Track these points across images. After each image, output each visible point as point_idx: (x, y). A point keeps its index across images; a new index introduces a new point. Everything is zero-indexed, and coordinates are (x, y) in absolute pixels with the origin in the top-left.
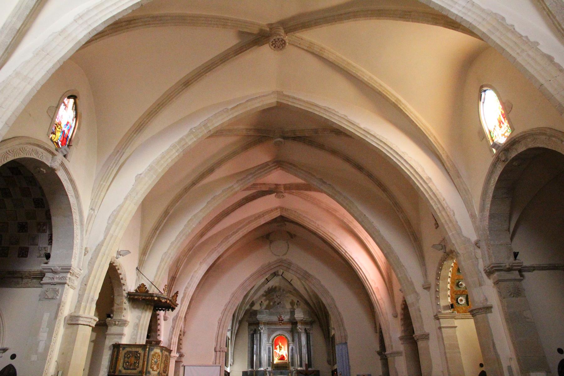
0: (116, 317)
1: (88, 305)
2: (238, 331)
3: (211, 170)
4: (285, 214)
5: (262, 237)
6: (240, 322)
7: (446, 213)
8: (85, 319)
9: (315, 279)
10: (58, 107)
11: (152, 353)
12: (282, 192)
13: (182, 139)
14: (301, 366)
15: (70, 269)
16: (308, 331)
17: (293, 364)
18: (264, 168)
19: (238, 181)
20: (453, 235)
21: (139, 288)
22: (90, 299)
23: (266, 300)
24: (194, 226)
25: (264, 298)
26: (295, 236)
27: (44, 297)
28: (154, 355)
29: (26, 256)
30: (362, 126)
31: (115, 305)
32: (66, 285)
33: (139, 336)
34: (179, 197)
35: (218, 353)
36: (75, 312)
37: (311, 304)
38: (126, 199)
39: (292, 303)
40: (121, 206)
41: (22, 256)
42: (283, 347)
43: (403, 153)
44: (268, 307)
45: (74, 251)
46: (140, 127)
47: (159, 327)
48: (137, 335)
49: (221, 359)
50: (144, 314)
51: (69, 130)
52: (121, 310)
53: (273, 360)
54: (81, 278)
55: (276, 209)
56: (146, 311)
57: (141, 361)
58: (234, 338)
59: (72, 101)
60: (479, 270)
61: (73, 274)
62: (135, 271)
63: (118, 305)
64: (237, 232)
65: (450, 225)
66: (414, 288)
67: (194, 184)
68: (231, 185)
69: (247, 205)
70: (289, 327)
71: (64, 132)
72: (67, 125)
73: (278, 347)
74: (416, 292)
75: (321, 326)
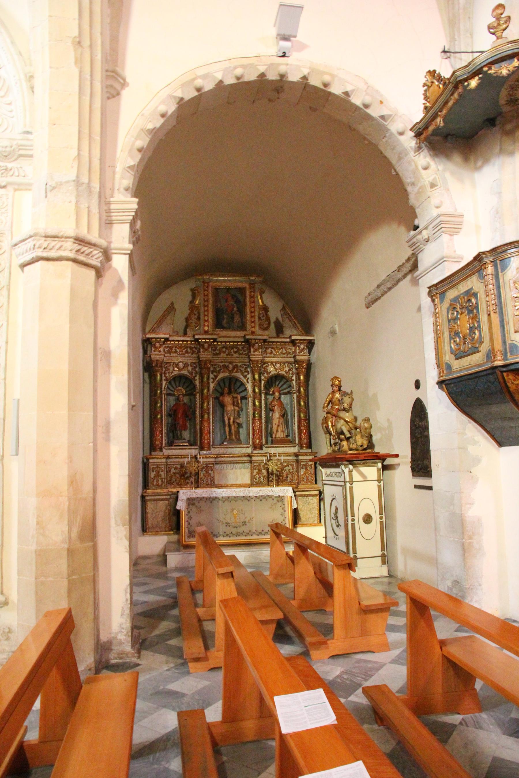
57: (484, 318)
63: (413, 184)
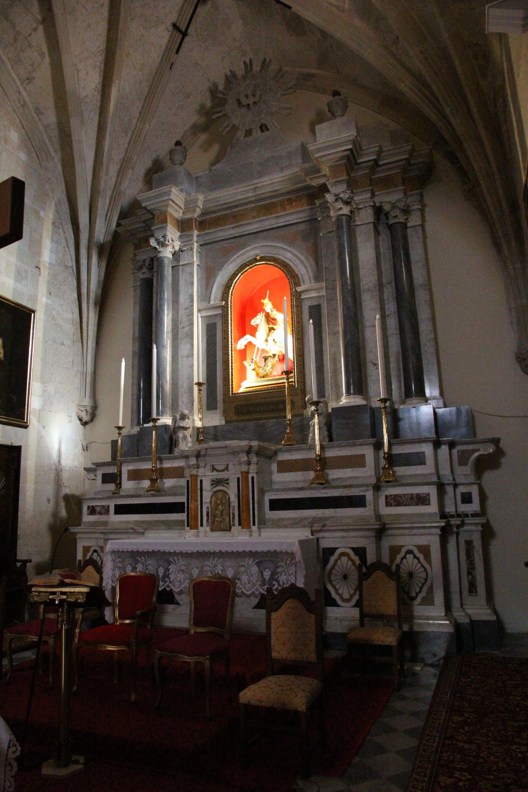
6: (111, 252)
23: (207, 146)
25: (203, 137)
37: (405, 86)
58: (91, 317)
73: (259, 320)
75: (472, 194)
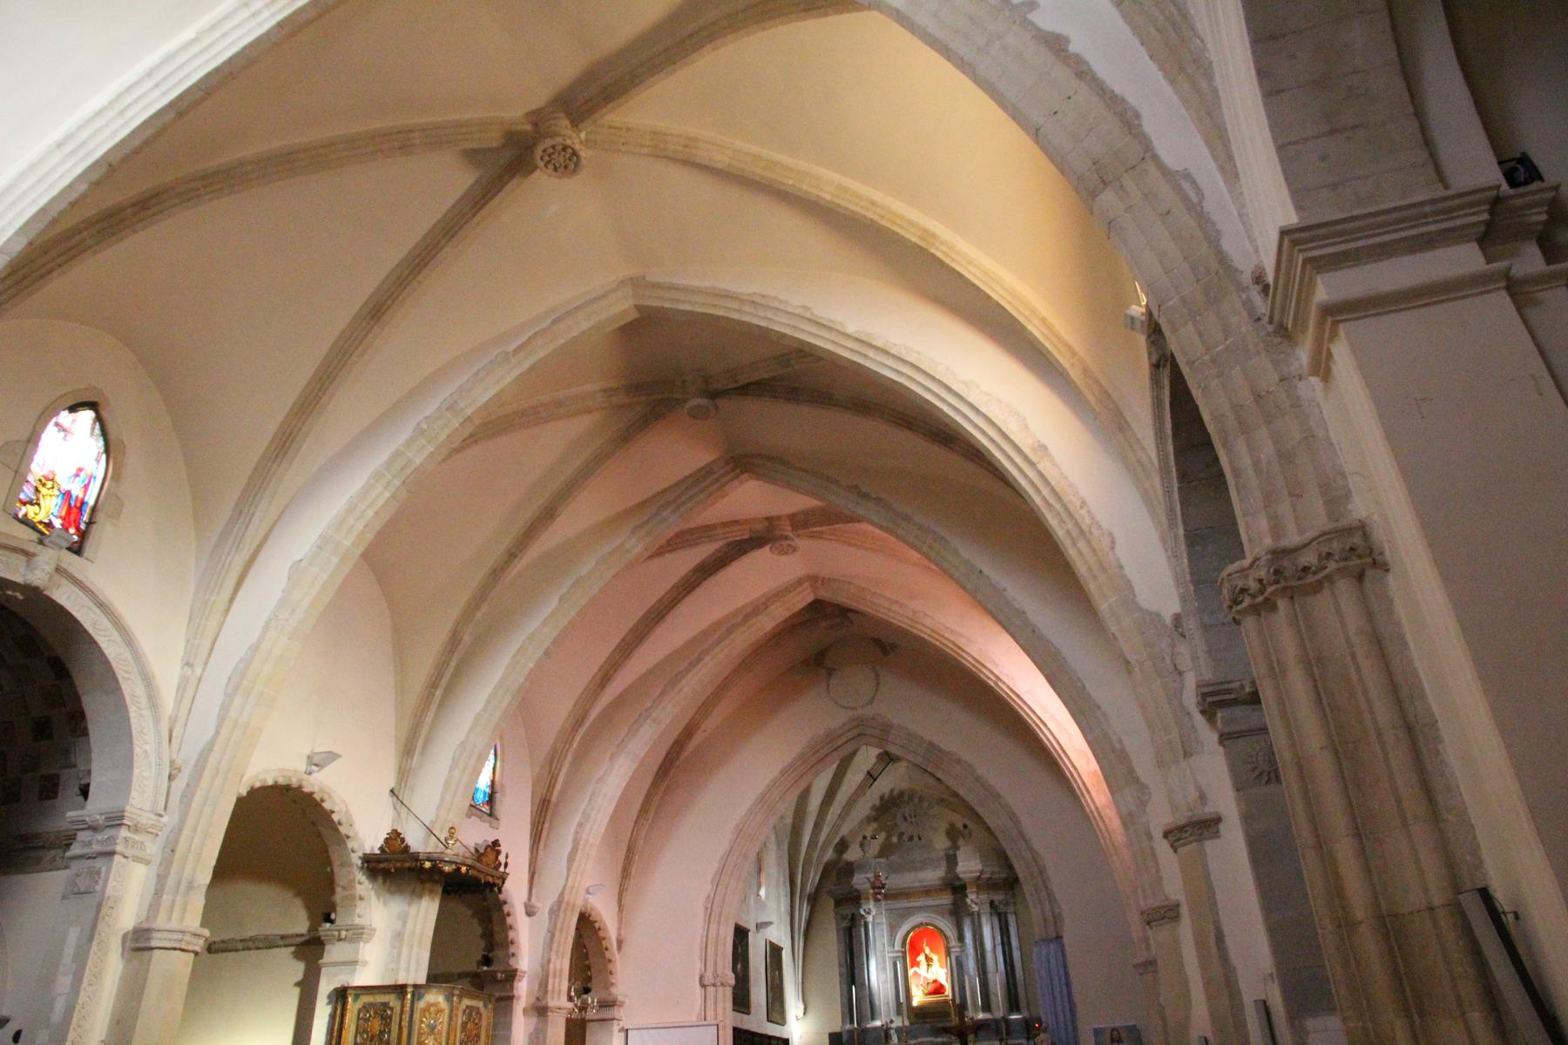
0: (340, 918)
1: (179, 899)
2: (809, 922)
3: (548, 514)
4: (824, 594)
5: (806, 662)
6: (814, 900)
7: (1089, 542)
8: (166, 935)
9: (959, 761)
10: (33, 440)
11: (421, 1004)
12: (786, 538)
13: (397, 455)
14: (987, 1007)
15: (122, 817)
16: (1002, 908)
17: (962, 1007)
18: (702, 482)
19: (633, 532)
20: (1111, 608)
21: (386, 840)
22: (183, 888)
24: (531, 665)
25: (875, 825)
26: (894, 647)
27: (76, 892)
28: (425, 1010)
29: (54, 795)
30: (851, 328)
31: (338, 890)
32: (117, 858)
33: (403, 965)
34: (481, 596)
35: (711, 990)
36: (148, 919)
38: (266, 627)
39: (953, 834)
40: (254, 649)
41: (49, 798)
42: (935, 957)
43: (966, 384)
44: (886, 850)
45: (136, 771)
46: (284, 444)
47: (511, 934)
48: (398, 962)
49: (720, 1005)
50: (413, 910)
51: (86, 487)
52: (352, 899)
53: (909, 997)
54: (163, 835)
55: (800, 582)
56: (420, 897)
57: (395, 1028)
58: (800, 944)
59: (87, 416)
60: (1182, 707)
61: (136, 829)
62: (387, 800)
64: (699, 660)
65: (1102, 578)
66: (1131, 771)
67: (511, 556)
68: (618, 542)
69: (708, 584)
70: (946, 899)
71: (68, 495)
72: (77, 475)
73: (921, 958)
74: (1137, 780)
